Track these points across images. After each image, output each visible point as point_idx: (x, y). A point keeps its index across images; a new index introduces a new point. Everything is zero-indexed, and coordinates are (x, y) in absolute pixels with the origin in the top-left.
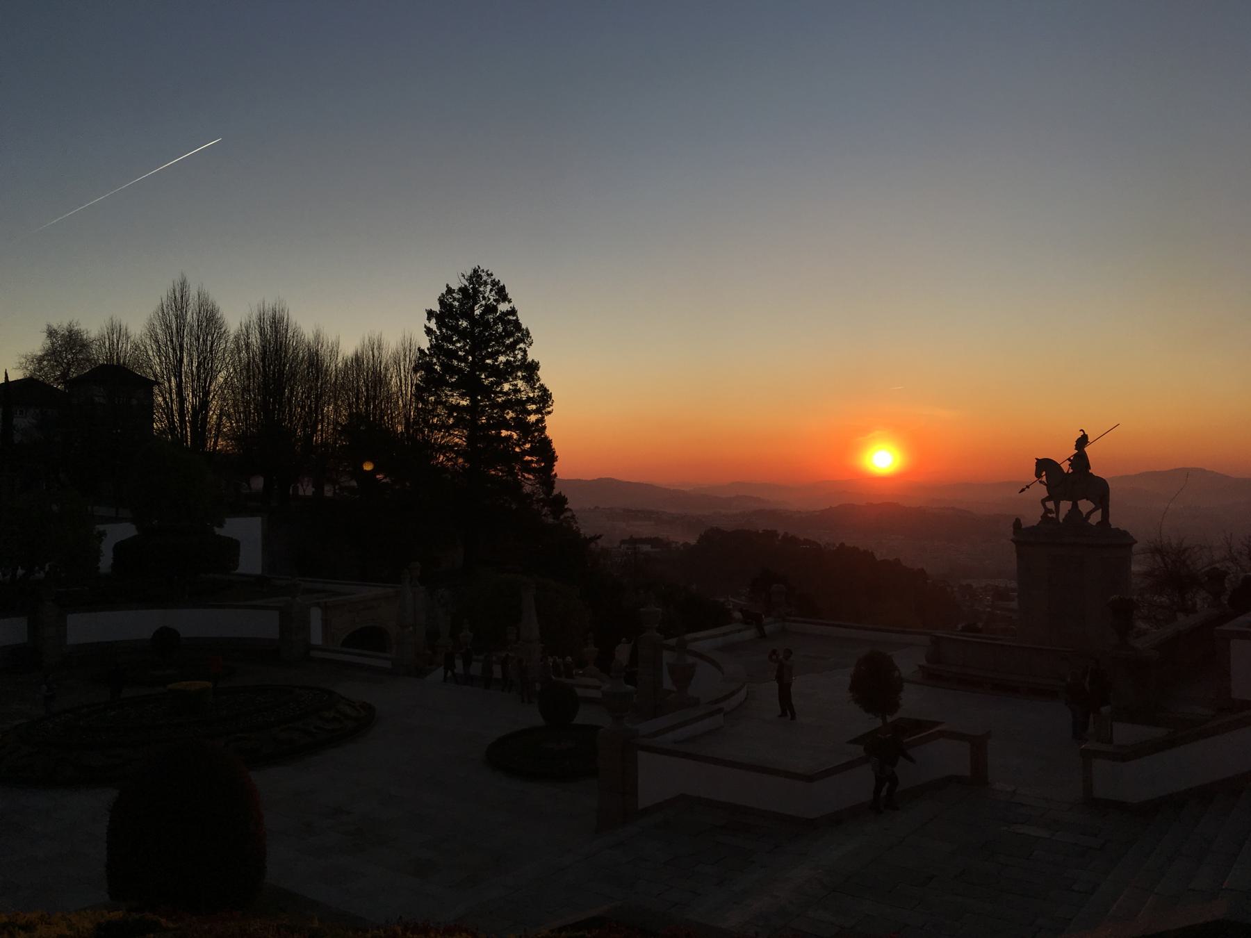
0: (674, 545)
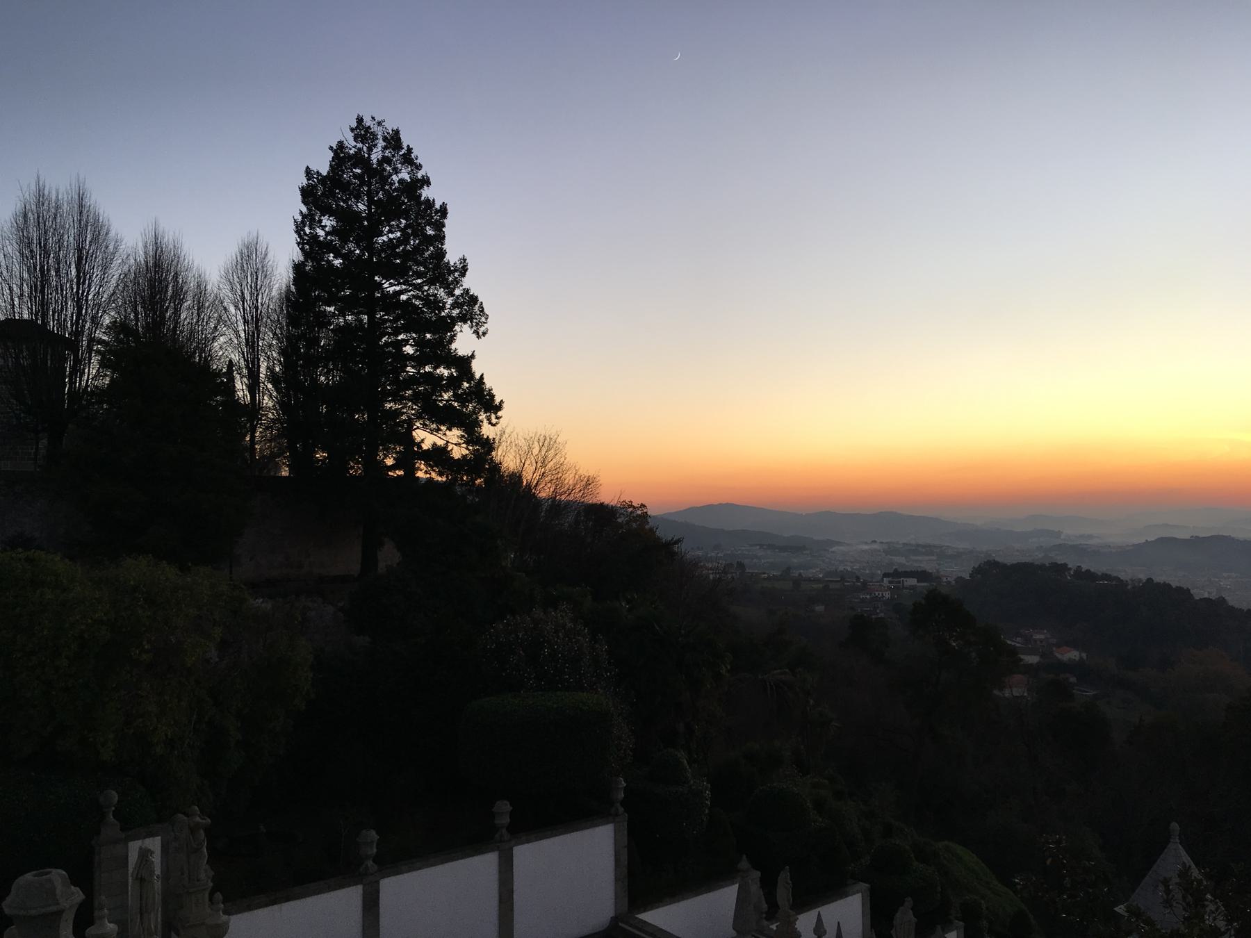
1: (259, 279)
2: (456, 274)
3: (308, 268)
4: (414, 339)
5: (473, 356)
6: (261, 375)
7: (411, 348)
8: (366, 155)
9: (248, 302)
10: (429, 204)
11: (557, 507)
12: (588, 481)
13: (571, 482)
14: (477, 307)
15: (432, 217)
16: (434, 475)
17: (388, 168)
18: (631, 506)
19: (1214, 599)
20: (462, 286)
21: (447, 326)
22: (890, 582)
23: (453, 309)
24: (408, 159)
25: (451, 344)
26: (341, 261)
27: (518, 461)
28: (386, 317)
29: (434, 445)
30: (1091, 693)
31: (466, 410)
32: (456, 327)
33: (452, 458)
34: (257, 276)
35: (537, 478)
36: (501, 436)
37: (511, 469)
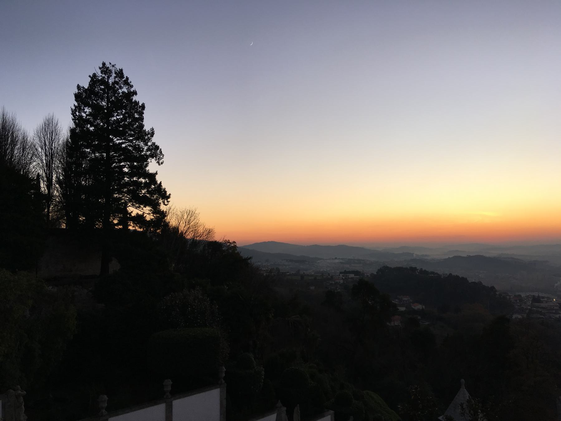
0: (366, 275)
1: (53, 135)
2: (149, 136)
3: (77, 131)
4: (128, 165)
5: (156, 173)
6: (53, 181)
7: (127, 169)
8: (107, 80)
9: (48, 146)
10: (136, 103)
11: (195, 243)
12: (209, 231)
13: (201, 231)
14: (158, 151)
15: (138, 109)
16: (137, 228)
17: (117, 86)
18: (229, 242)
19: (477, 282)
20: (152, 141)
21: (144, 159)
22: (343, 276)
23: (147, 151)
24: (127, 83)
25: (146, 168)
26: (94, 128)
27: (177, 222)
28: (115, 155)
29: (137, 214)
30: (427, 323)
31: (153, 198)
32: (149, 160)
33: (146, 220)
34: (52, 134)
35: (186, 229)
36: (169, 210)
37: (174, 225)
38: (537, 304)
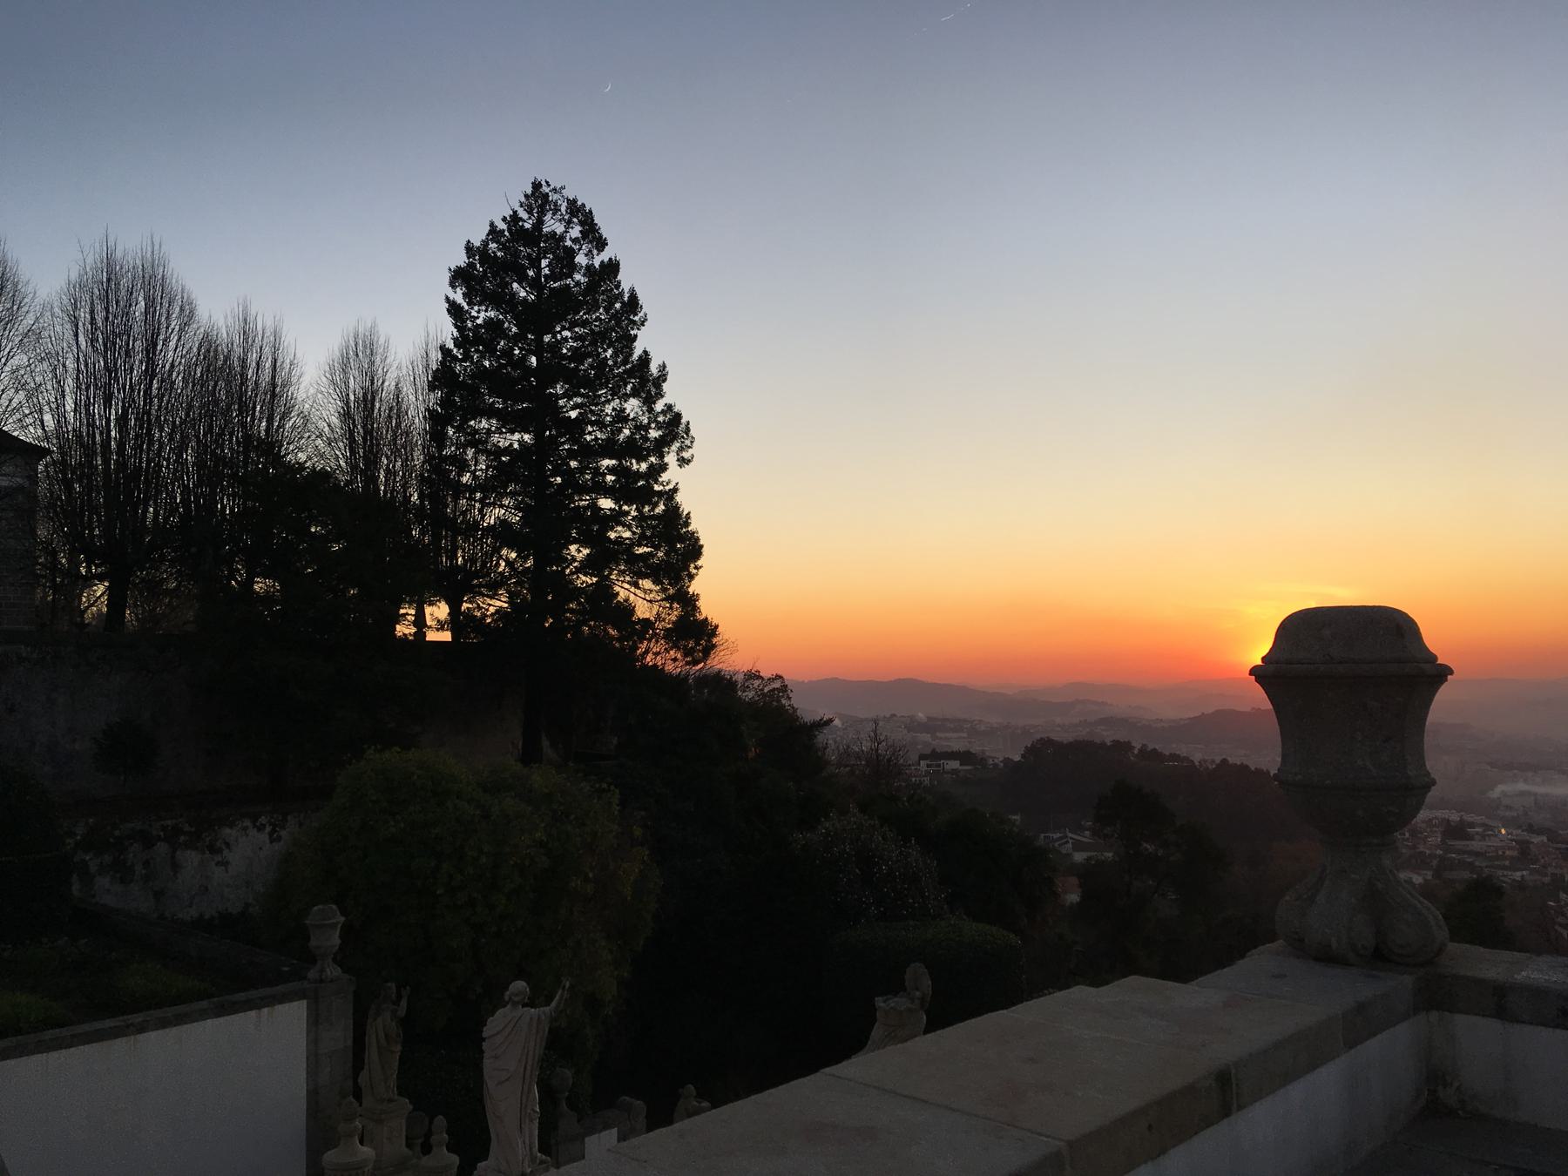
0: (991, 762)
38: (1459, 844)
